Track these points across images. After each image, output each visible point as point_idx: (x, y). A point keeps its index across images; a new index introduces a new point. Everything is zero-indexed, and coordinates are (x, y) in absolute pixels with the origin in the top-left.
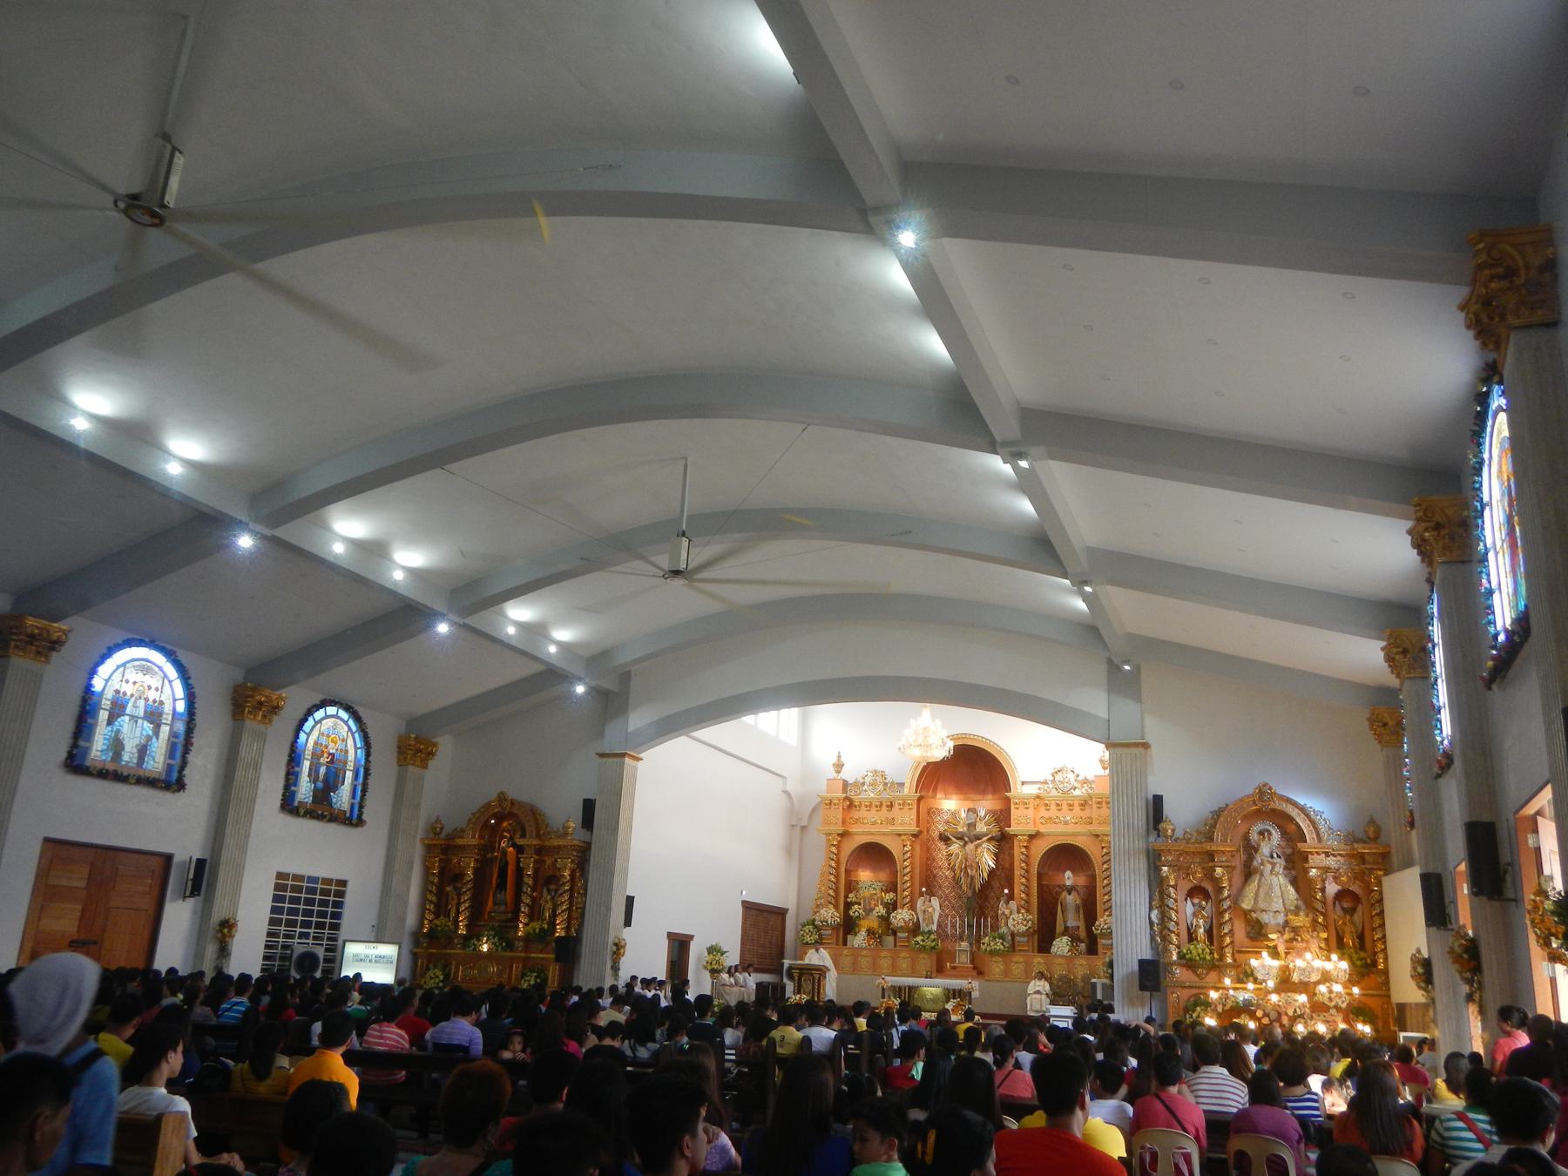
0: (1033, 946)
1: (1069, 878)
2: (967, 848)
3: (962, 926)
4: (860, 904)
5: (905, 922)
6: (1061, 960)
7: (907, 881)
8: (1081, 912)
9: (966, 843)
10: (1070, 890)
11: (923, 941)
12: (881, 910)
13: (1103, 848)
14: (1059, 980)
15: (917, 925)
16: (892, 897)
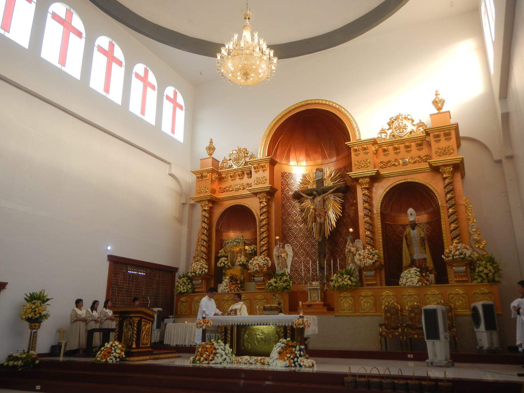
0: (381, 280)
1: (411, 215)
2: (315, 200)
3: (314, 270)
4: (227, 257)
5: (260, 266)
6: (412, 292)
7: (263, 232)
8: (427, 245)
9: (315, 197)
10: (413, 225)
11: (276, 282)
12: (242, 259)
13: (445, 179)
14: (411, 312)
15: (273, 268)
16: (252, 248)
